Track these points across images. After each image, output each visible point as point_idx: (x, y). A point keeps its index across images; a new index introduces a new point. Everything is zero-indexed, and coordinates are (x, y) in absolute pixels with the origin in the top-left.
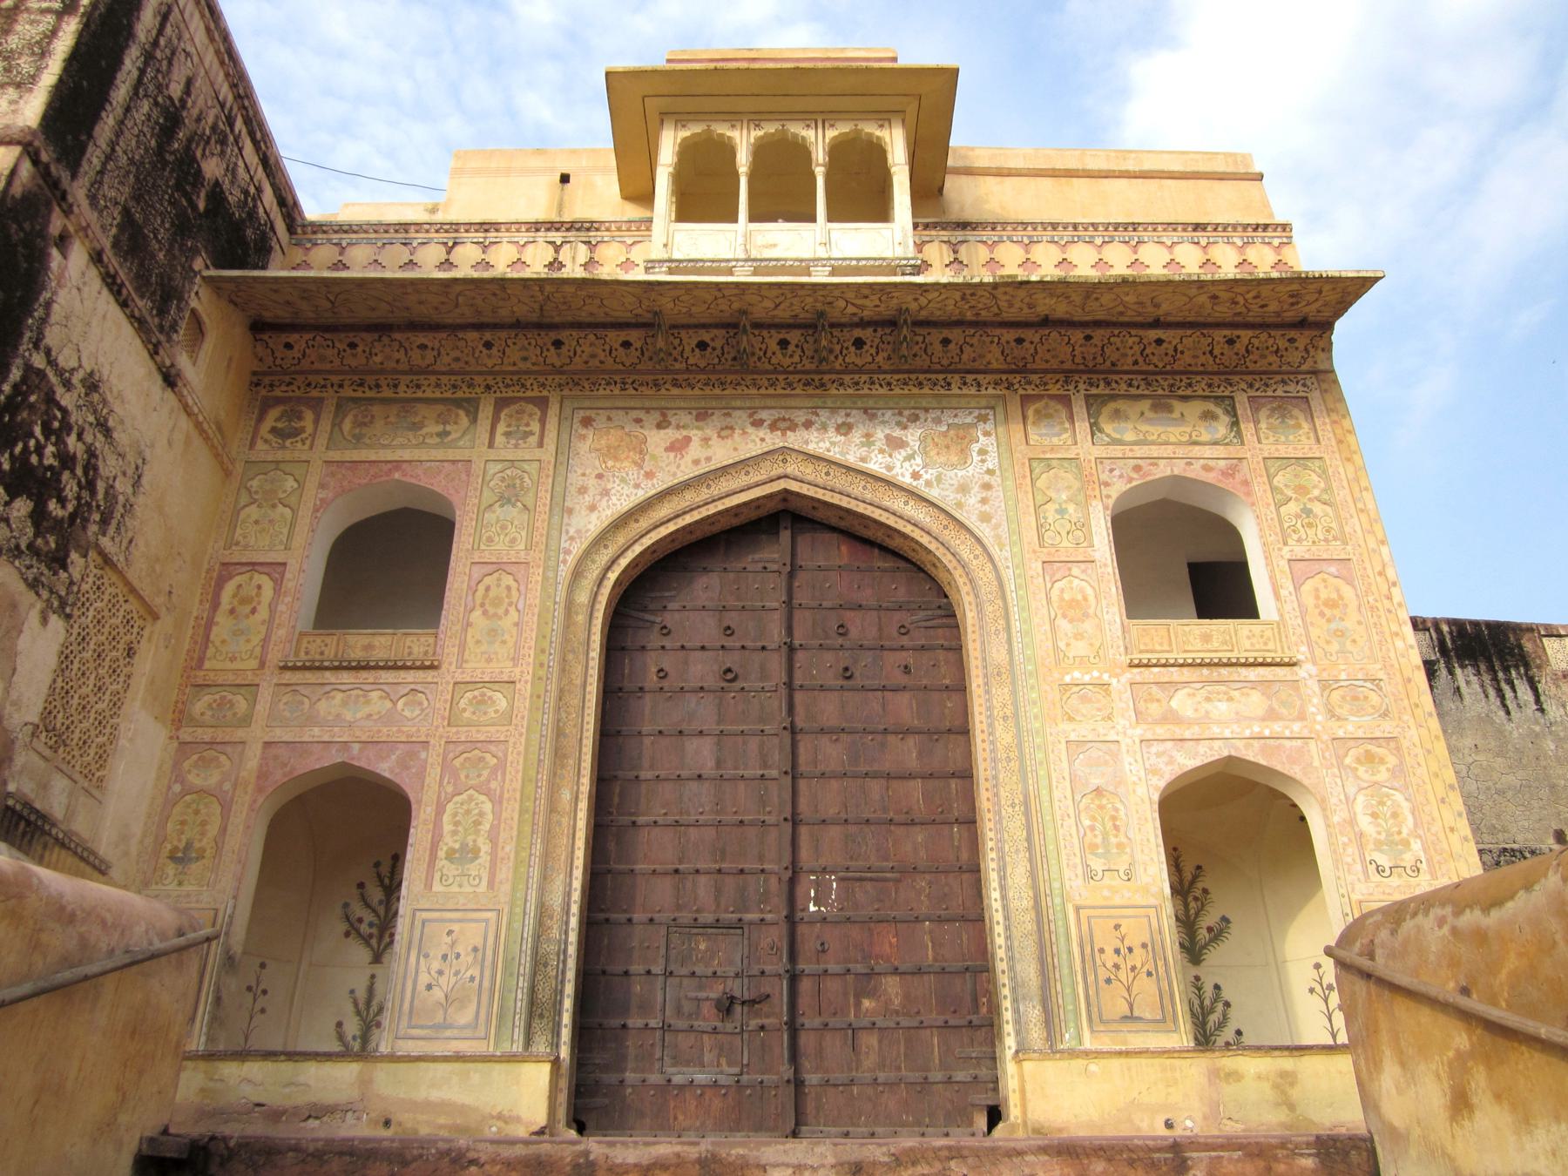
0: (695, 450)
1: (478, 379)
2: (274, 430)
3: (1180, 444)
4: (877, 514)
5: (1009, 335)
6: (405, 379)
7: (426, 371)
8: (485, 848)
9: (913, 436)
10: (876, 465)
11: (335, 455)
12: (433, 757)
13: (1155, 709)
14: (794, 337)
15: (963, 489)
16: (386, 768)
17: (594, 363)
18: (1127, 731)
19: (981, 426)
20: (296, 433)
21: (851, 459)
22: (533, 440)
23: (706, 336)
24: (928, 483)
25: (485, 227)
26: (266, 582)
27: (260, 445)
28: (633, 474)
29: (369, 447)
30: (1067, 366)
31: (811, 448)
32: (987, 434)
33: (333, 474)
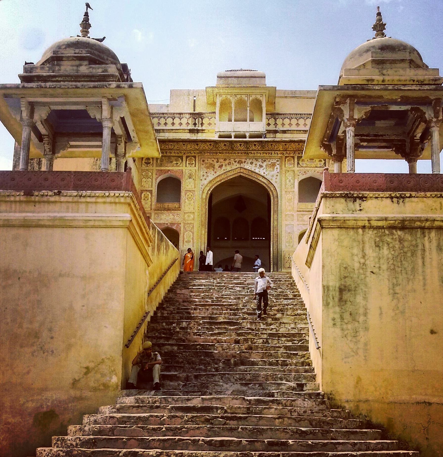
0: (224, 167)
1: (182, 151)
2: (145, 162)
3: (314, 167)
4: (257, 180)
5: (284, 144)
6: (168, 151)
7: (172, 150)
8: (192, 241)
9: (264, 165)
10: (257, 171)
11: (158, 168)
12: (182, 226)
13: (301, 219)
14: (242, 144)
15: (273, 176)
16: (174, 227)
17: (204, 148)
18: (295, 223)
19: (277, 163)
20: (150, 163)
21: (253, 170)
22: (194, 165)
23: (226, 143)
24: (266, 175)
25: (180, 114)
26: (149, 193)
27: (143, 166)
28: (213, 172)
29: (163, 166)
30: (295, 150)
31: (245, 167)
32: (278, 164)
33: (158, 172)
